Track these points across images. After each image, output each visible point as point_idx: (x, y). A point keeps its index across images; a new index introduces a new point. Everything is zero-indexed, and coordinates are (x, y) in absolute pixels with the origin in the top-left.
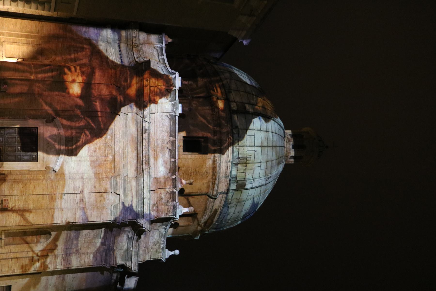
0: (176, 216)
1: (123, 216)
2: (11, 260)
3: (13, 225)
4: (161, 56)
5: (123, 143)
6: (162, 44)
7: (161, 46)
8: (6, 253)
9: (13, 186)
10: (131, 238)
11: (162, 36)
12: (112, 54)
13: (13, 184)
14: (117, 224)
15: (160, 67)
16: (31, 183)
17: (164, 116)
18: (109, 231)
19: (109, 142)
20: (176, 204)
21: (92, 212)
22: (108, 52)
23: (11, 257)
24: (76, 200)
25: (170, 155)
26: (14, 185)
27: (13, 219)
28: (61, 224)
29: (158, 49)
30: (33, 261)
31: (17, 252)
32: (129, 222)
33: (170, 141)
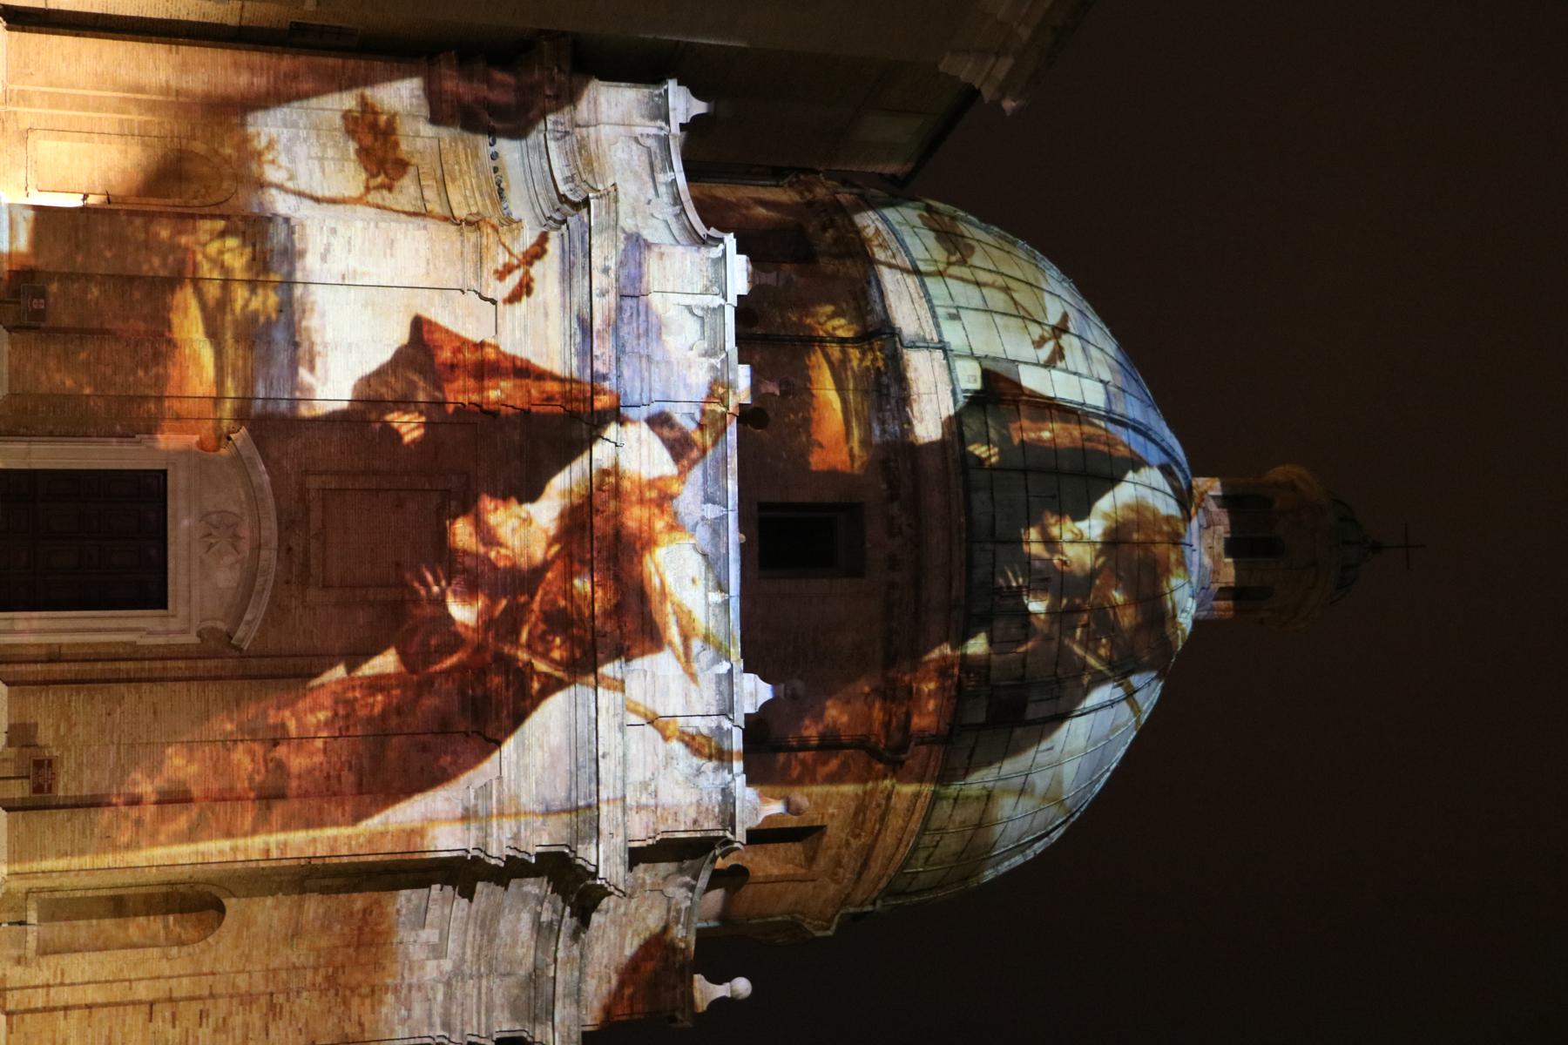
0: (733, 833)
2: (62, 1013)
3: (72, 868)
6: (668, 122)
7: (662, 133)
8: (43, 987)
9: (69, 706)
10: (551, 923)
11: (666, 91)
13: (69, 701)
14: (490, 864)
15: (660, 216)
16: (140, 697)
18: (460, 894)
20: (734, 779)
22: (447, 162)
23: (63, 1004)
26: (73, 704)
27: (72, 841)
28: (262, 864)
29: (651, 143)
30: (151, 1021)
31: (88, 983)
32: (538, 855)
33: (703, 518)
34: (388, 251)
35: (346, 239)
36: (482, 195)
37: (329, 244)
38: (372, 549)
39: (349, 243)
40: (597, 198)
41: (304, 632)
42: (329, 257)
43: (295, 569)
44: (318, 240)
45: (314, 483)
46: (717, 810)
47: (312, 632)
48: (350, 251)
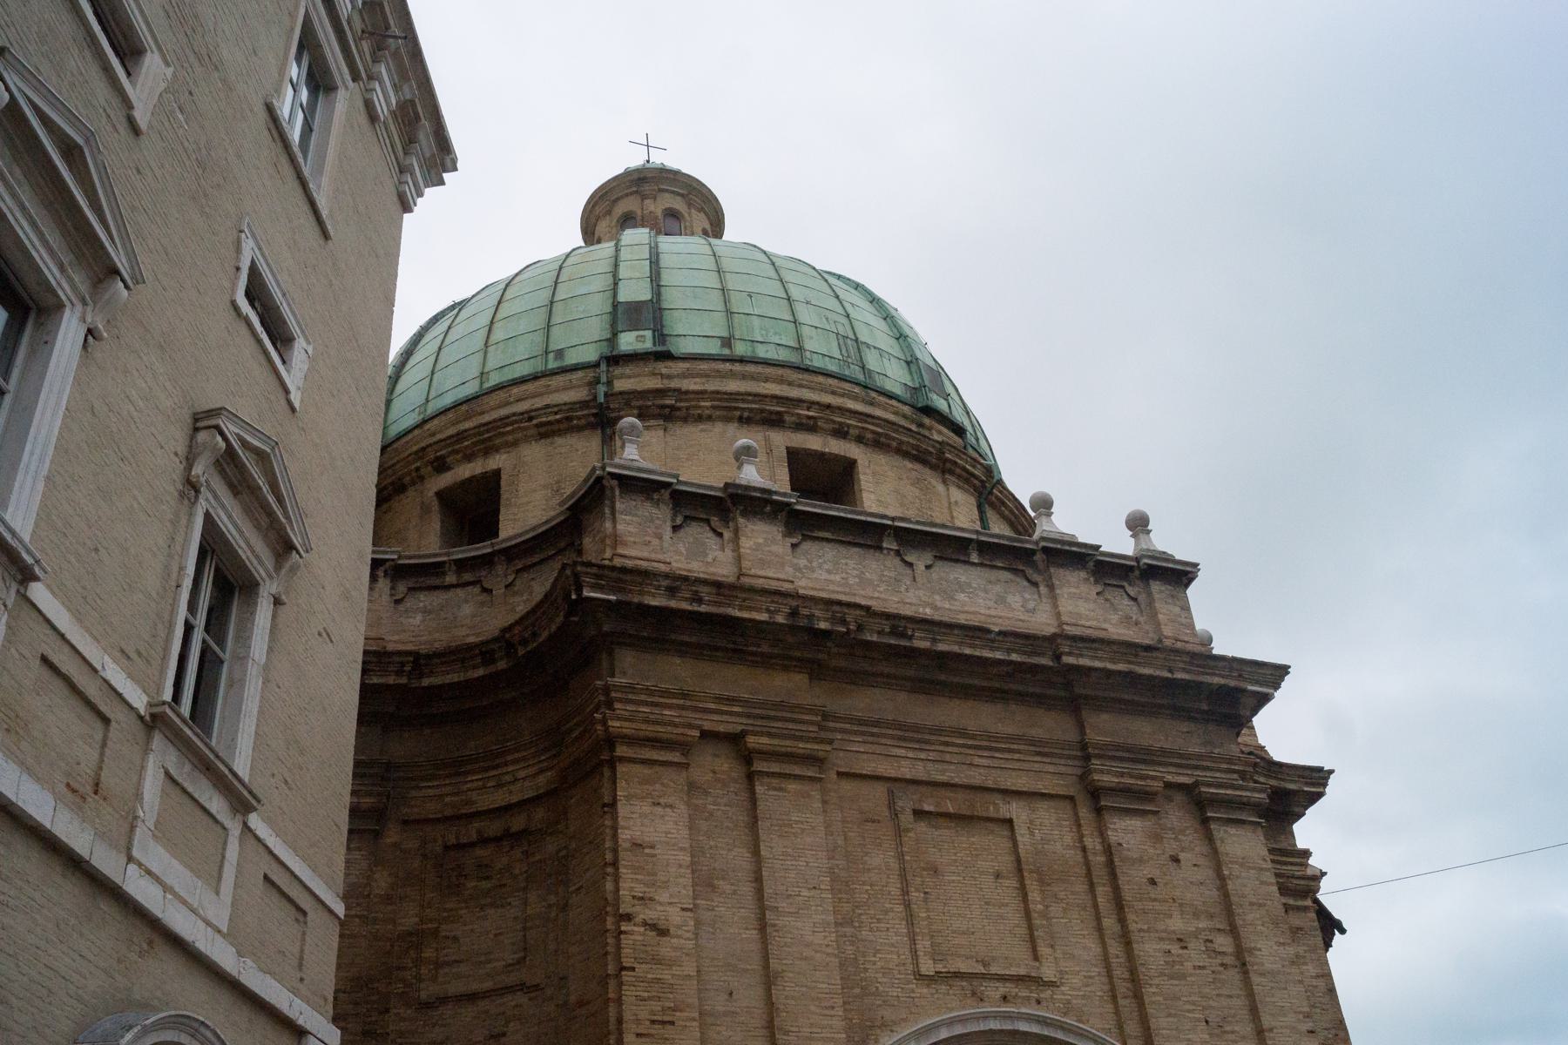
1: (1235, 776)
4: (444, 574)
5: (947, 744)
12: (448, 789)
17: (795, 561)
19: (951, 810)
21: (1252, 904)
24: (1213, 972)
25: (957, 561)
33: (898, 553)
34: (647, 851)
35: (636, 902)
36: (497, 767)
37: (645, 924)
38: (987, 903)
39: (642, 898)
40: (579, 590)
41: (1087, 986)
42: (662, 925)
43: (1024, 993)
44: (640, 938)
45: (927, 967)
46: (1169, 587)
47: (1085, 977)
48: (651, 899)
